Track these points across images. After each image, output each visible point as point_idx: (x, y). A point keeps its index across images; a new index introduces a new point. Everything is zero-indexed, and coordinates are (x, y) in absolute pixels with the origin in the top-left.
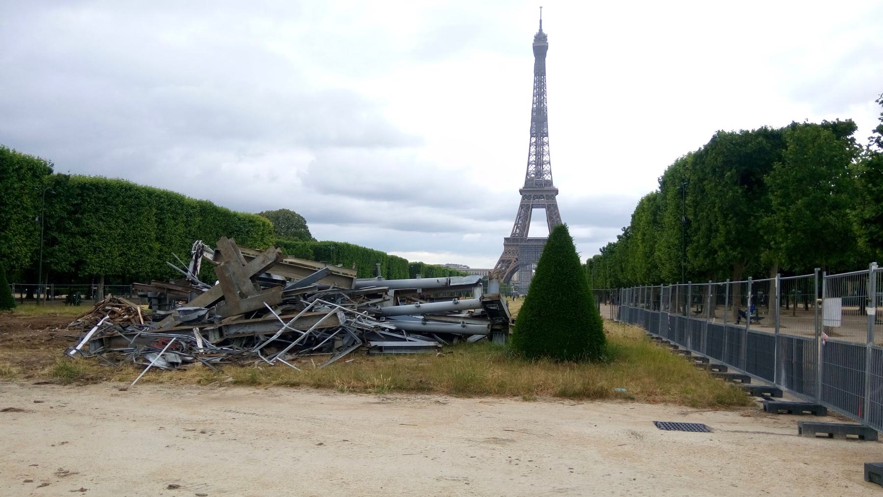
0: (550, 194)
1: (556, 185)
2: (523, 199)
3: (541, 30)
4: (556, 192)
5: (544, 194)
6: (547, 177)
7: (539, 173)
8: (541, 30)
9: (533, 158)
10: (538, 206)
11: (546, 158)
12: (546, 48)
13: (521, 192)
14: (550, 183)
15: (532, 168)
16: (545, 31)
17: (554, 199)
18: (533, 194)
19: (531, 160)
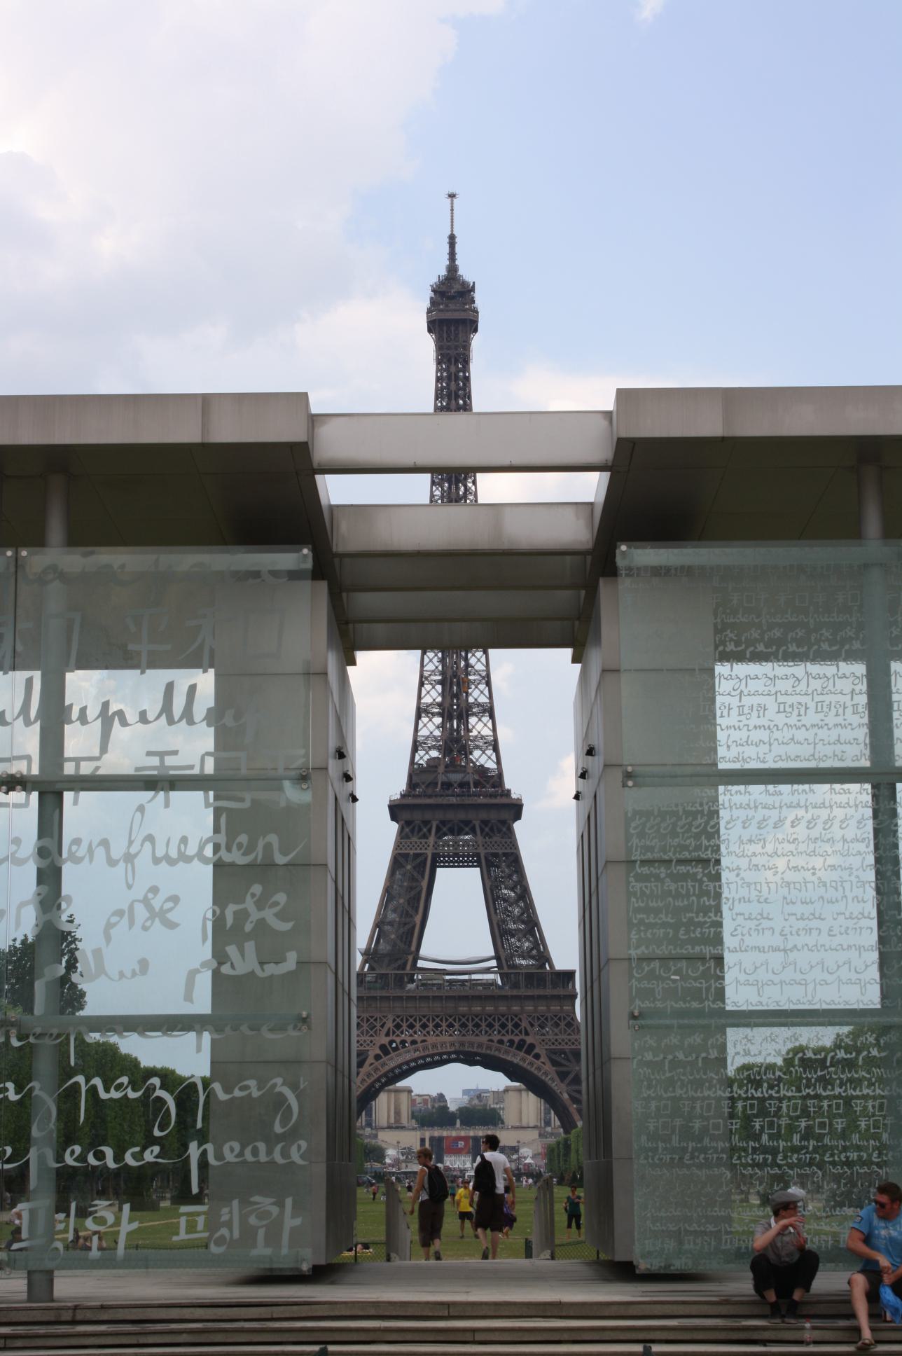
0: (493, 816)
1: (514, 783)
2: (401, 835)
3: (452, 268)
4: (516, 809)
5: (476, 818)
6: (482, 758)
7: (455, 744)
8: (452, 268)
9: (433, 695)
10: (457, 860)
11: (477, 695)
12: (471, 325)
13: (396, 810)
14: (493, 780)
15: (432, 726)
16: (466, 272)
17: (510, 833)
18: (435, 819)
19: (427, 700)
